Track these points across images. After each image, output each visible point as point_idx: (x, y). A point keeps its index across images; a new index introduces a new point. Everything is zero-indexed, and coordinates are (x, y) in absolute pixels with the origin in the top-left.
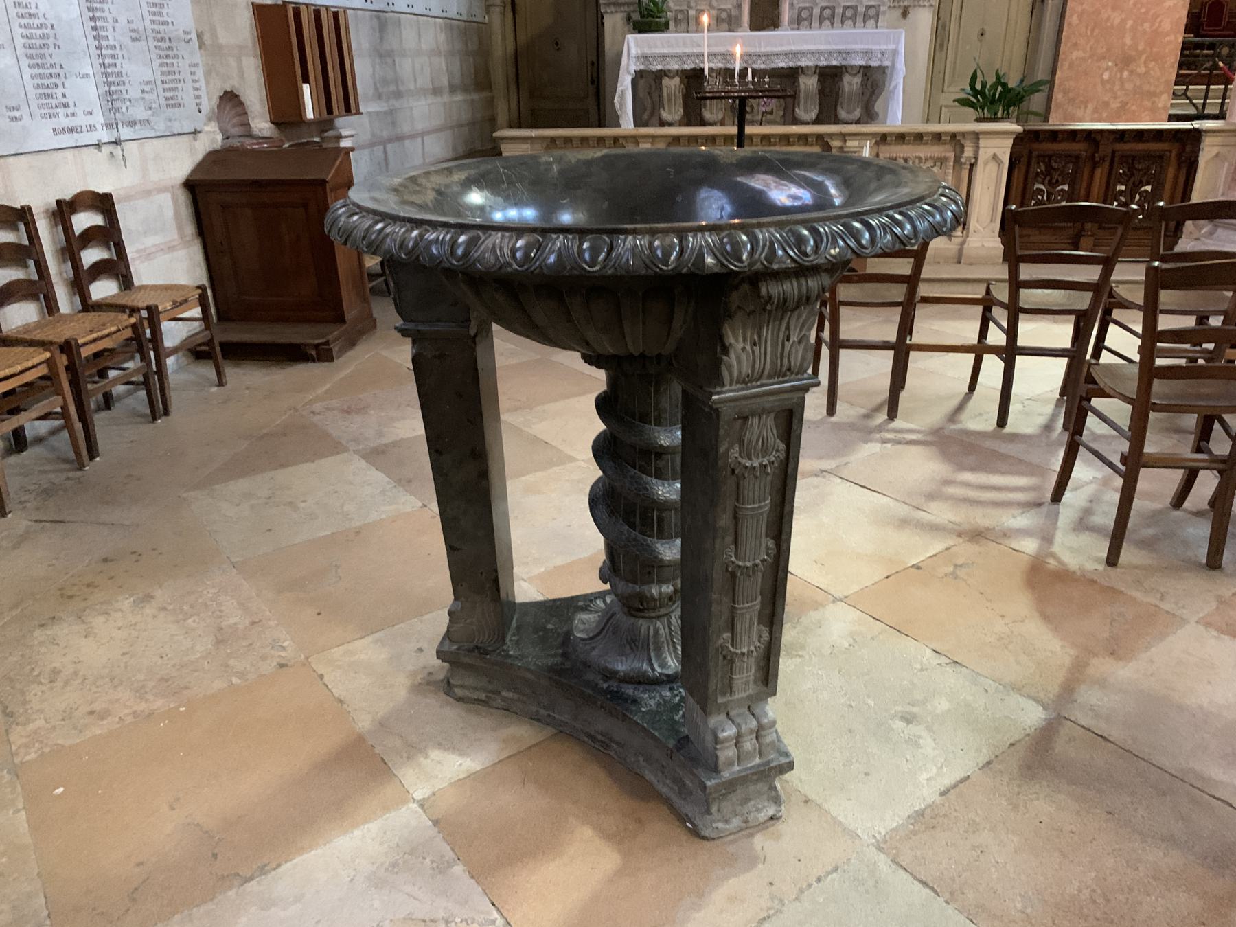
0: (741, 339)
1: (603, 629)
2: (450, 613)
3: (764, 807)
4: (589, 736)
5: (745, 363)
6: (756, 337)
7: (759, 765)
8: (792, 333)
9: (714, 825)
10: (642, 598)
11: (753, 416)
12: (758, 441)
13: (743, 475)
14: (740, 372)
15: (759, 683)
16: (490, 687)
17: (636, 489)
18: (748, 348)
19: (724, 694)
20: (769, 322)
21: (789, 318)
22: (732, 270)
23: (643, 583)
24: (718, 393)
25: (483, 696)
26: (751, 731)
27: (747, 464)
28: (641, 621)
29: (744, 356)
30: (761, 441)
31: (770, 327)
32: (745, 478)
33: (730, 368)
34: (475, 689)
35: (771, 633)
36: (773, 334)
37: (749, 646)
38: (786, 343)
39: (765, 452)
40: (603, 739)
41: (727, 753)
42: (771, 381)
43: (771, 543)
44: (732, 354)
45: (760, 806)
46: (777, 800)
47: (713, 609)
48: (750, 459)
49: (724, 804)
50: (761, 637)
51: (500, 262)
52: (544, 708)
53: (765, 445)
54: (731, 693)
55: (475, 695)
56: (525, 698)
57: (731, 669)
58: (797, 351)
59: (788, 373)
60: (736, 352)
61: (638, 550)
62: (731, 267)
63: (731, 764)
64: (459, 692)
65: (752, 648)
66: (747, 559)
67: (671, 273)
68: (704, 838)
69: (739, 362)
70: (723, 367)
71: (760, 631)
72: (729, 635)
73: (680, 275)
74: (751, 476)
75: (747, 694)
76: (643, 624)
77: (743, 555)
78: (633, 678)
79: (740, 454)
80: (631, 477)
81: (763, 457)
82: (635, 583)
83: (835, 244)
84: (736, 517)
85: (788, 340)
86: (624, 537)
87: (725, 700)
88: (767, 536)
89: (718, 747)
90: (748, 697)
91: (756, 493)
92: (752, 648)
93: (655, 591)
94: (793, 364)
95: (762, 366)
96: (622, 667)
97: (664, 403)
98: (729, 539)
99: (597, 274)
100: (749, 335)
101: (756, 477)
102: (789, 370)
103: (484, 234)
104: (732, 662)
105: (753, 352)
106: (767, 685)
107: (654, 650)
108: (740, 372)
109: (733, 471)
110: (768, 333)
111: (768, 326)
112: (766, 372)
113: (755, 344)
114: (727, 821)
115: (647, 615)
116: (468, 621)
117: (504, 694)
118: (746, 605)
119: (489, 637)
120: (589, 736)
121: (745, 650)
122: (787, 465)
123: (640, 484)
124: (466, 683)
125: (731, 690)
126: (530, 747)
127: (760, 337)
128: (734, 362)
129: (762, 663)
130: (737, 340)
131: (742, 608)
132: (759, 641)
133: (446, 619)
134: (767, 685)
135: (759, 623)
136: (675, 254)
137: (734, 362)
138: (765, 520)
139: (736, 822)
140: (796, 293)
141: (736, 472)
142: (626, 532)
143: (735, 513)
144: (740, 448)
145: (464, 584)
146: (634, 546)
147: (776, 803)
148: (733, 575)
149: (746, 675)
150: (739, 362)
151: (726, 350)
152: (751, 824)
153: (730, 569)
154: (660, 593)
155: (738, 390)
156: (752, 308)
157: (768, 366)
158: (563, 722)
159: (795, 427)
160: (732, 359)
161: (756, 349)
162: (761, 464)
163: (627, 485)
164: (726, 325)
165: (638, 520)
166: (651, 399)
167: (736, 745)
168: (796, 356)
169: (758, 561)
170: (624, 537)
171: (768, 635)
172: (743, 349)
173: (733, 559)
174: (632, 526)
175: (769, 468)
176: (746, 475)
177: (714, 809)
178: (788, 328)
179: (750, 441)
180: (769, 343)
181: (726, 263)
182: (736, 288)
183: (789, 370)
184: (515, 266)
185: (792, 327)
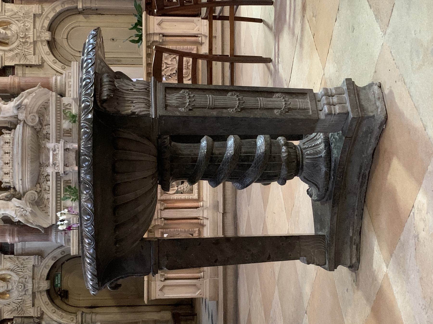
0: (130, 108)
1: (313, 183)
2: (308, 264)
3: (373, 91)
4: (361, 186)
5: (140, 106)
6: (130, 102)
7: (349, 96)
8: (130, 89)
9: (379, 113)
10: (289, 161)
11: (165, 102)
12: (177, 100)
13: (193, 106)
14: (144, 107)
15: (305, 97)
16: (349, 243)
17: (228, 163)
18: (134, 105)
19: (309, 112)
20: (123, 97)
21: (123, 89)
22: (92, 108)
23: (281, 161)
24: (152, 116)
25: (354, 247)
26: (327, 99)
27: (188, 104)
28: (304, 163)
29: (137, 106)
30: (177, 99)
31: (126, 97)
32: (194, 105)
33: (141, 111)
34: (351, 251)
35: (277, 92)
36: (129, 96)
37: (282, 102)
38: (134, 90)
39: (183, 97)
40: (361, 178)
41: (337, 109)
42: (151, 97)
43: (230, 94)
44: (135, 111)
45: (373, 93)
46: (371, 85)
47: (259, 117)
48: (186, 103)
49: (369, 110)
50: (278, 97)
51: (89, 198)
52: (354, 211)
53: (180, 97)
54: (308, 109)
55: (355, 251)
56: (351, 223)
57: (295, 109)
58: (137, 86)
59: (148, 89)
60: (135, 109)
61: (260, 162)
62: (91, 108)
63: (344, 107)
64: (354, 260)
65: (283, 100)
66: (235, 103)
67: (92, 131)
68: (386, 118)
69: (139, 108)
70: (141, 114)
71: (275, 98)
72: (275, 110)
73: (93, 127)
74: (194, 102)
75: (309, 102)
76: (306, 161)
77: (233, 105)
78: (327, 164)
79: (183, 107)
80: (223, 166)
81: (186, 98)
82: (281, 165)
83: (89, 72)
84: (214, 108)
85: (133, 90)
86: (254, 169)
87: (311, 112)
88: (226, 96)
89: (333, 113)
90: (311, 101)
91: (203, 100)
92: (283, 100)
93: (284, 155)
94: (143, 88)
95: (142, 99)
96: (324, 169)
97: (186, 152)
98: (224, 111)
99: (92, 159)
100: (128, 105)
101: (195, 100)
102: (146, 89)
103: (82, 208)
104: (290, 109)
105: (136, 103)
106: (306, 93)
107: (317, 155)
108: (144, 107)
109: (190, 110)
110: (128, 97)
111: (125, 97)
112: (146, 98)
113: (133, 102)
114: (377, 108)
115: (301, 160)
116: (312, 254)
117: (351, 235)
118: (259, 103)
119: (321, 243)
120: (361, 186)
121: (284, 103)
122: (191, 88)
123: (226, 161)
124: (349, 256)
125: (306, 109)
126: (370, 217)
127: (129, 100)
128: (139, 110)
129: (294, 96)
130: (130, 109)
131: (261, 105)
132: (281, 97)
133: (311, 265)
134: (306, 93)
135: (272, 98)
136: (87, 130)
137: (139, 110)
138: (216, 96)
139: (378, 103)
140: (108, 86)
141: (191, 108)
142: (252, 168)
143: (211, 109)
144: (180, 107)
145: (289, 254)
146: (258, 164)
147: (372, 86)
148: (242, 109)
149: (299, 103)
150: (139, 108)
151: (133, 113)
152: (381, 96)
153: (239, 110)
154: (285, 152)
155: (152, 108)
156: (116, 103)
157: (143, 97)
158: (358, 200)
159: (174, 86)
160: (137, 111)
161: (134, 102)
162: (188, 99)
163: (226, 167)
164: (122, 113)
165: (246, 163)
166: (185, 157)
167: (334, 105)
168: (139, 86)
169: (237, 99)
170: (254, 169)
171: (278, 94)
172: (134, 106)
173: (234, 109)
174: (249, 166)
175: (191, 95)
176: (193, 104)
177: (371, 114)
178: (127, 90)
179: (177, 103)
180: (133, 97)
181: (90, 110)
182: (105, 108)
183: (146, 89)
184: (90, 192)
185: (127, 89)
